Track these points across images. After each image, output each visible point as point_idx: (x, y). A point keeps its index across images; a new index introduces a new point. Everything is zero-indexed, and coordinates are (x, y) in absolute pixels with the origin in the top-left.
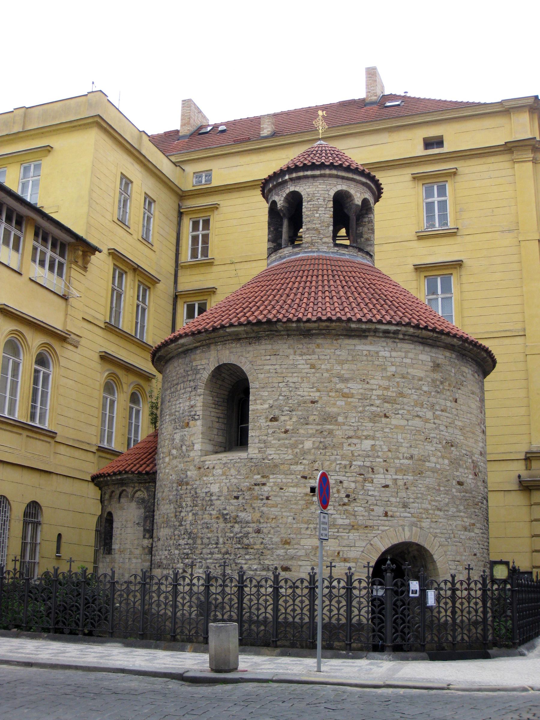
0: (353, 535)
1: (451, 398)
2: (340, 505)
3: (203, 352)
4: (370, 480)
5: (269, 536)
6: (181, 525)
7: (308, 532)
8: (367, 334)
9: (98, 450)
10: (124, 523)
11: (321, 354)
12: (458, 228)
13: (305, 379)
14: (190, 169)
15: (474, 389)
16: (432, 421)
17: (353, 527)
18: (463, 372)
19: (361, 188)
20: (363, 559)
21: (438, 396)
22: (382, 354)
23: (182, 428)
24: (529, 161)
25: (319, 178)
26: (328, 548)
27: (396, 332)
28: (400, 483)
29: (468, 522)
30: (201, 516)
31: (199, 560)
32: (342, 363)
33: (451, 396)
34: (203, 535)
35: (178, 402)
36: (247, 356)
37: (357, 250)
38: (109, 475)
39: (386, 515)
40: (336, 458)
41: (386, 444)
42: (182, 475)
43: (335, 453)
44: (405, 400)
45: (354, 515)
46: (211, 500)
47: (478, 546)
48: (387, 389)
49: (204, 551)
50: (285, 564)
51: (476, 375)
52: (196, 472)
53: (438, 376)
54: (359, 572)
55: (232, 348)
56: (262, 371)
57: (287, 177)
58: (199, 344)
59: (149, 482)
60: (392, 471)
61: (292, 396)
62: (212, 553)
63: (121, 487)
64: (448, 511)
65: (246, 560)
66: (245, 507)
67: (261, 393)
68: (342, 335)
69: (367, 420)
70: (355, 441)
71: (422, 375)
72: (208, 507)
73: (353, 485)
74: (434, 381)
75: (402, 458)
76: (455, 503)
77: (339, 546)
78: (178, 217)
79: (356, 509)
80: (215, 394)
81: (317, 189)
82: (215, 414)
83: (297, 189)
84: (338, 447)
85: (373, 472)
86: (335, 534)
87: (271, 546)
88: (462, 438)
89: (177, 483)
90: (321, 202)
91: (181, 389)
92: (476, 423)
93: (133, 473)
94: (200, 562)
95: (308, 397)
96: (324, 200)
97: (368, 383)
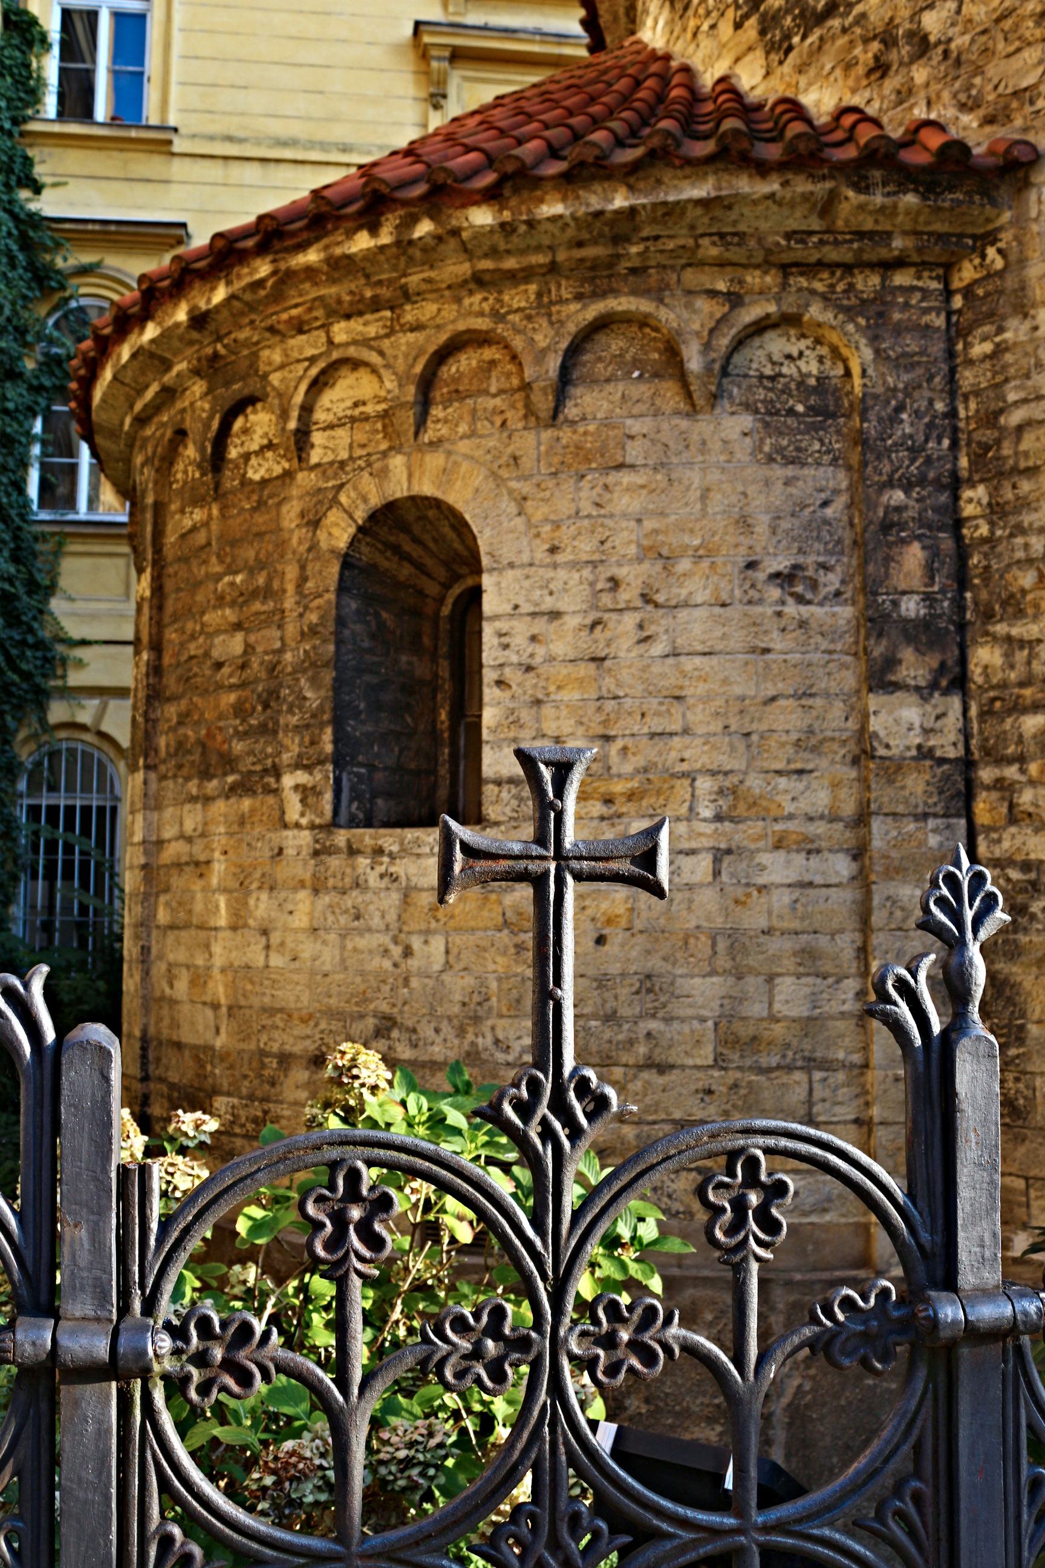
59: (888, 266)
63: (599, 294)
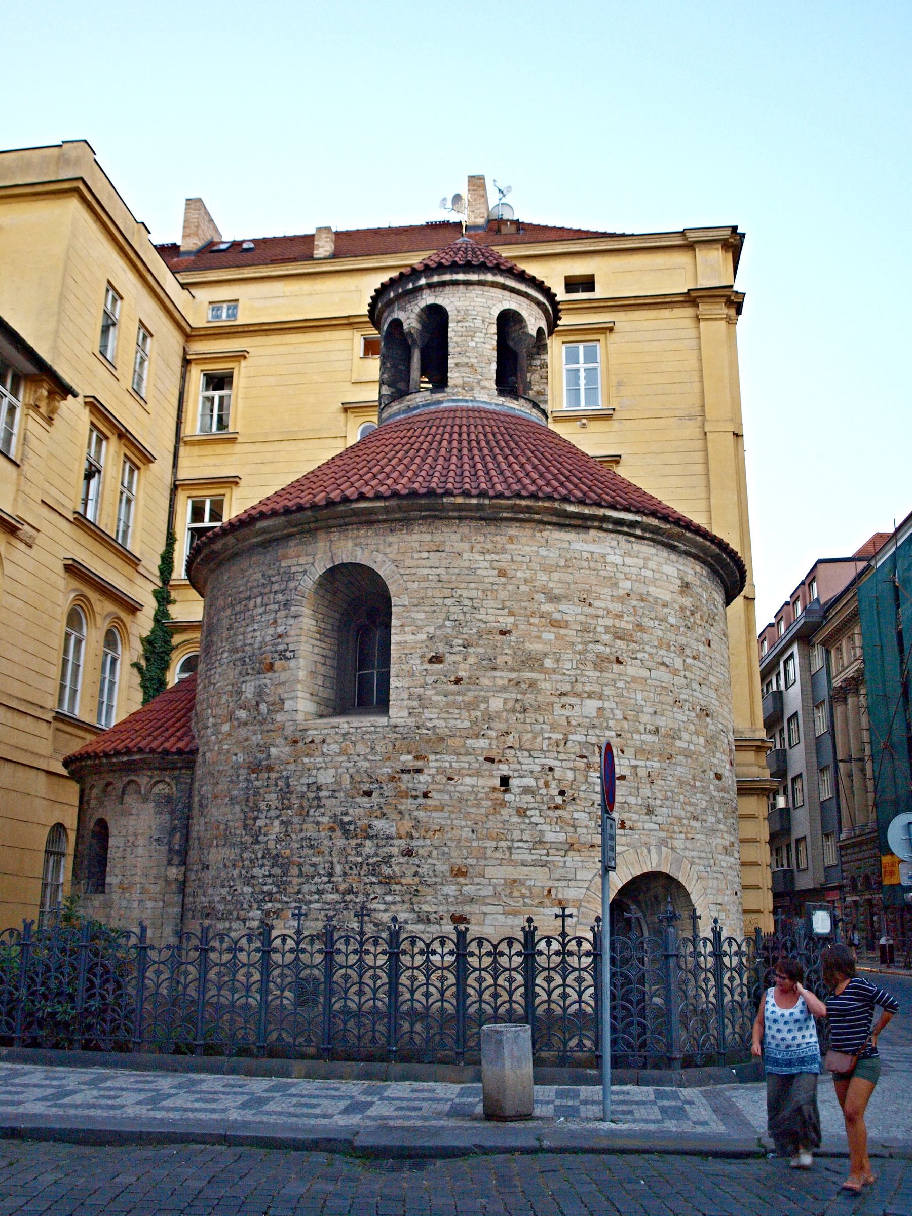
0: (573, 859)
2: (549, 808)
3: (302, 543)
5: (430, 861)
6: (257, 842)
7: (498, 855)
8: (589, 523)
9: (55, 718)
10: (131, 839)
11: (516, 552)
12: (614, 410)
13: (489, 593)
14: (204, 295)
16: (682, 673)
20: (588, 902)
21: (689, 634)
22: (610, 559)
23: (259, 673)
24: (721, 319)
25: (476, 287)
26: (532, 883)
27: (633, 524)
28: (642, 773)
30: (298, 826)
31: (294, 905)
32: (549, 569)
33: (703, 636)
34: (302, 860)
35: (250, 629)
36: (388, 550)
37: (531, 405)
38: (106, 755)
41: (620, 707)
42: (259, 755)
44: (646, 637)
45: (573, 826)
46: (318, 798)
48: (619, 616)
49: (305, 888)
50: (459, 910)
52: (287, 749)
53: (687, 602)
55: (358, 537)
56: (414, 578)
57: (423, 281)
58: (295, 529)
59: (181, 768)
61: (466, 622)
62: (320, 892)
63: (128, 775)
64: (706, 821)
65: (385, 903)
66: (385, 811)
67: (414, 615)
69: (590, 666)
72: (312, 811)
73: (570, 775)
74: (682, 609)
78: (183, 366)
79: (576, 815)
80: (320, 616)
81: (473, 304)
82: (321, 651)
83: (439, 301)
84: (545, 710)
87: (433, 879)
88: (717, 703)
89: (249, 767)
91: (255, 607)
93: (152, 751)
94: (296, 908)
95: (495, 624)
96: (483, 321)
97: (590, 605)
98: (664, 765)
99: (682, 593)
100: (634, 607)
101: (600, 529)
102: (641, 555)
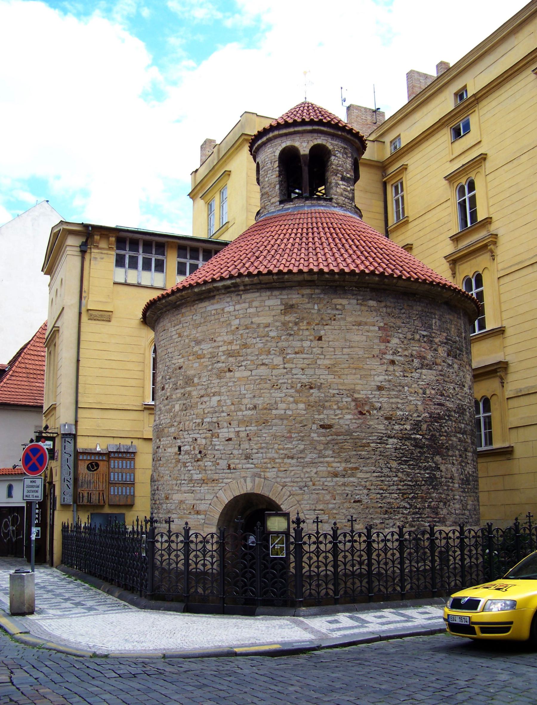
0: (204, 488)
1: (311, 338)
2: (195, 461)
4: (216, 435)
8: (212, 294)
15: (359, 319)
16: (282, 366)
17: (203, 482)
18: (336, 305)
19: (308, 137)
20: (210, 512)
21: (291, 338)
22: (227, 310)
25: (269, 143)
27: (236, 285)
28: (243, 435)
29: (340, 467)
39: (229, 468)
40: (193, 418)
43: (192, 413)
44: (249, 351)
45: (205, 470)
47: (366, 491)
48: (230, 343)
51: (372, 303)
54: (207, 524)
60: (235, 423)
64: (303, 458)
68: (197, 300)
69: (215, 376)
70: (205, 399)
71: (269, 321)
74: (284, 324)
75: (244, 409)
76: (315, 449)
77: (194, 499)
84: (194, 407)
85: (219, 426)
86: (193, 488)
90: (269, 165)
92: (366, 356)
97: (215, 341)
98: (260, 427)
99: (285, 314)
100: (241, 334)
101: (219, 294)
102: (247, 300)
